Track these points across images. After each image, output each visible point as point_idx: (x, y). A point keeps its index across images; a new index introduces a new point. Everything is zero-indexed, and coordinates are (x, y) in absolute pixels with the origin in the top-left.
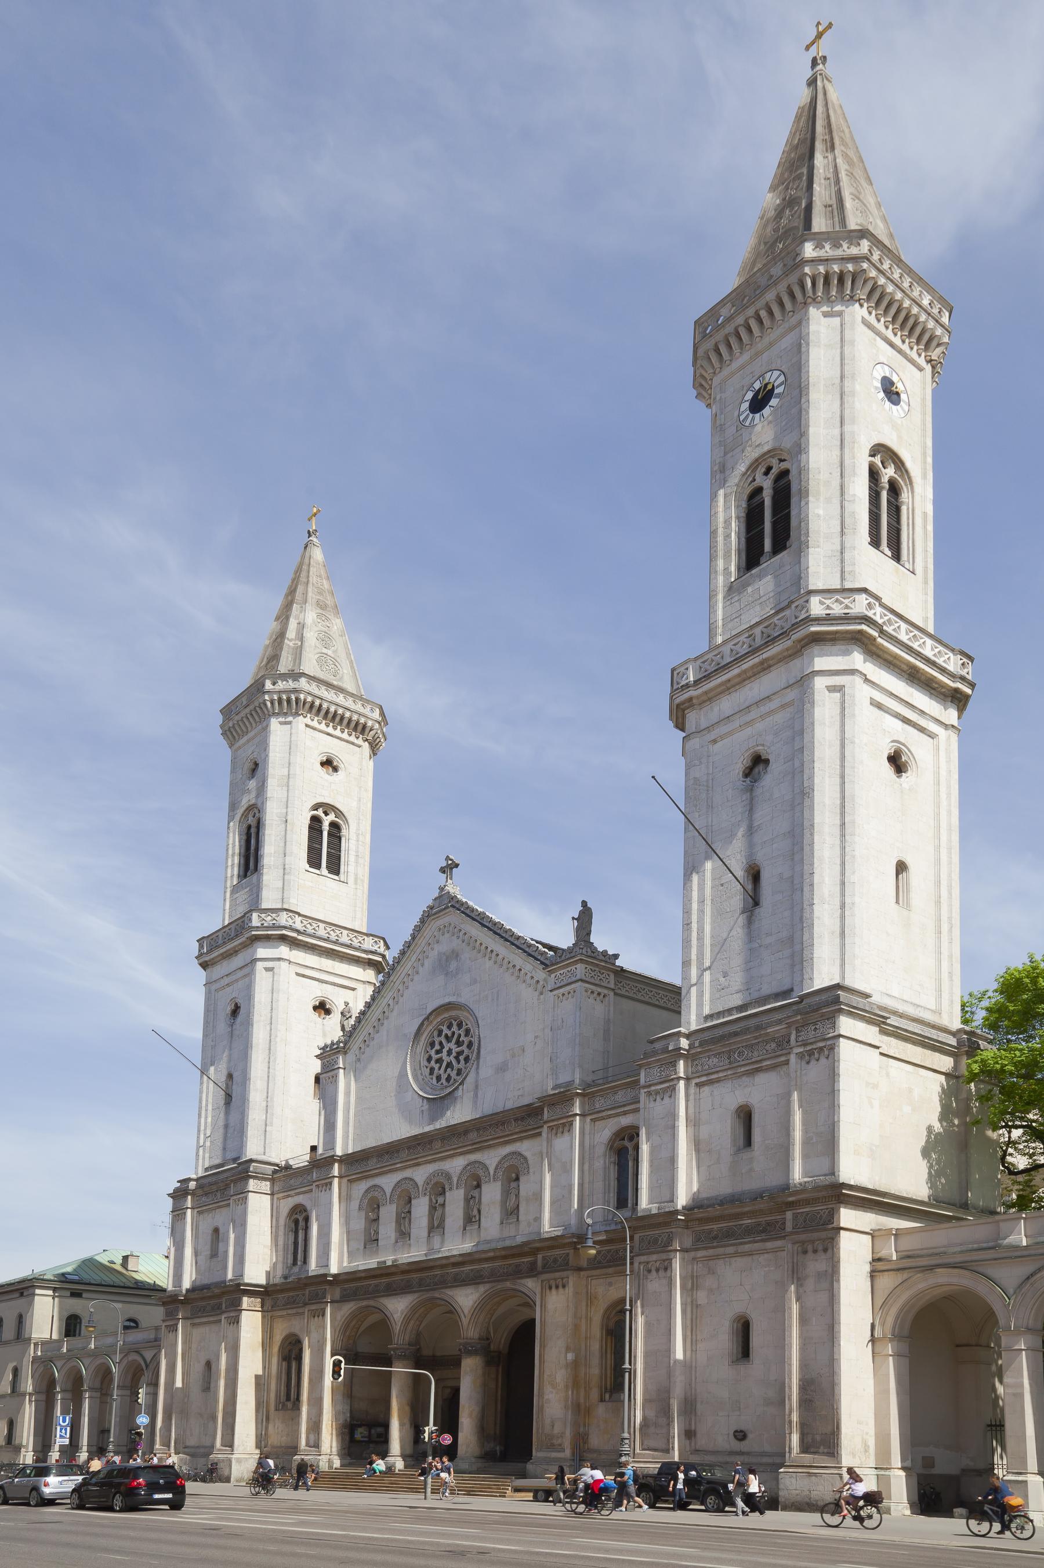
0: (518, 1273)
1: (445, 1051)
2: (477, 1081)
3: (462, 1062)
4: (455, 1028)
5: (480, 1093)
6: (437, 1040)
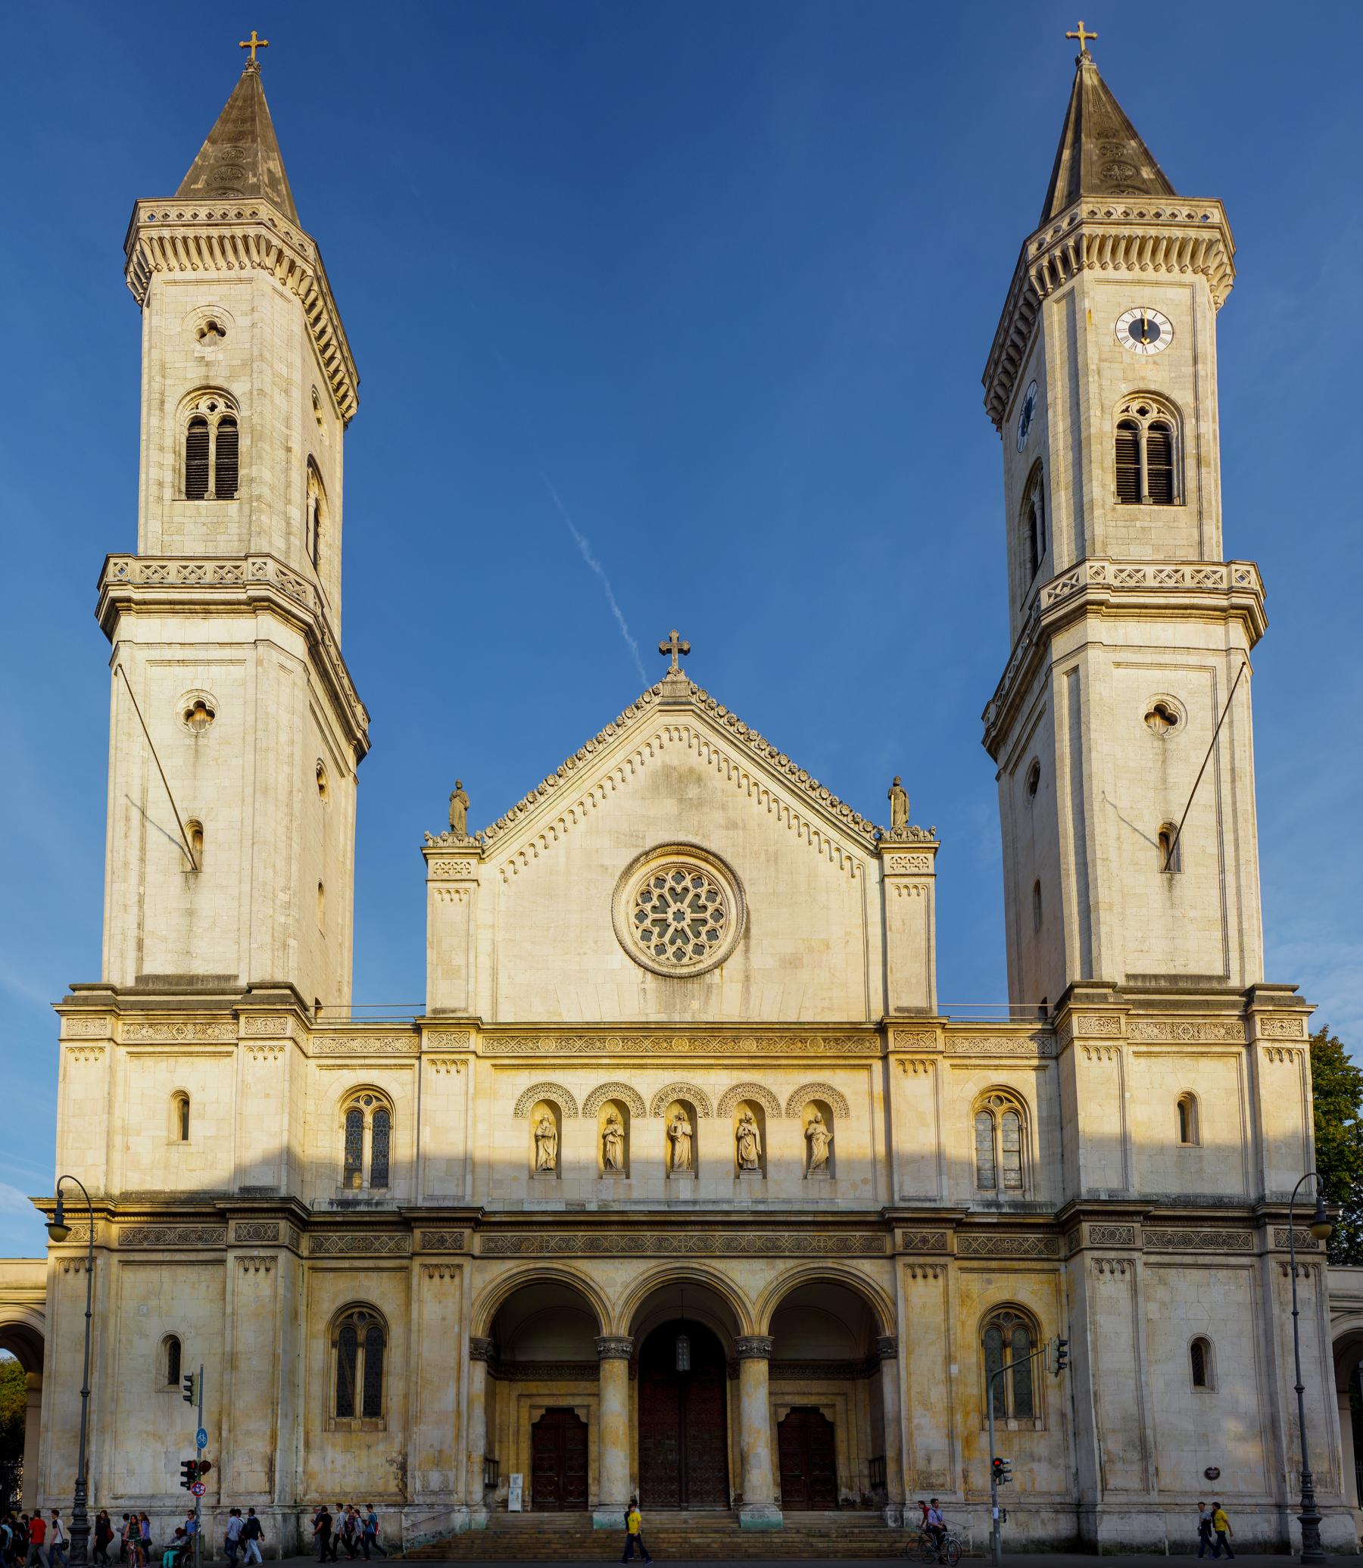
0: (844, 1250)
1: (671, 911)
2: (746, 970)
3: (704, 936)
4: (687, 882)
5: (753, 989)
6: (656, 892)
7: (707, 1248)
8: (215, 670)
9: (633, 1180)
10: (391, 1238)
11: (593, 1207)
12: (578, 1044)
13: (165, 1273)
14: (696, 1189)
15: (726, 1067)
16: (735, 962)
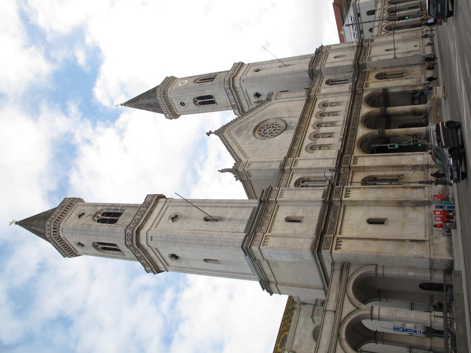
7: (356, 118)
8: (166, 213)
9: (336, 131)
10: (343, 175)
11: (342, 137)
12: (297, 142)
13: (345, 223)
14: (340, 121)
15: (311, 118)
16: (285, 119)
